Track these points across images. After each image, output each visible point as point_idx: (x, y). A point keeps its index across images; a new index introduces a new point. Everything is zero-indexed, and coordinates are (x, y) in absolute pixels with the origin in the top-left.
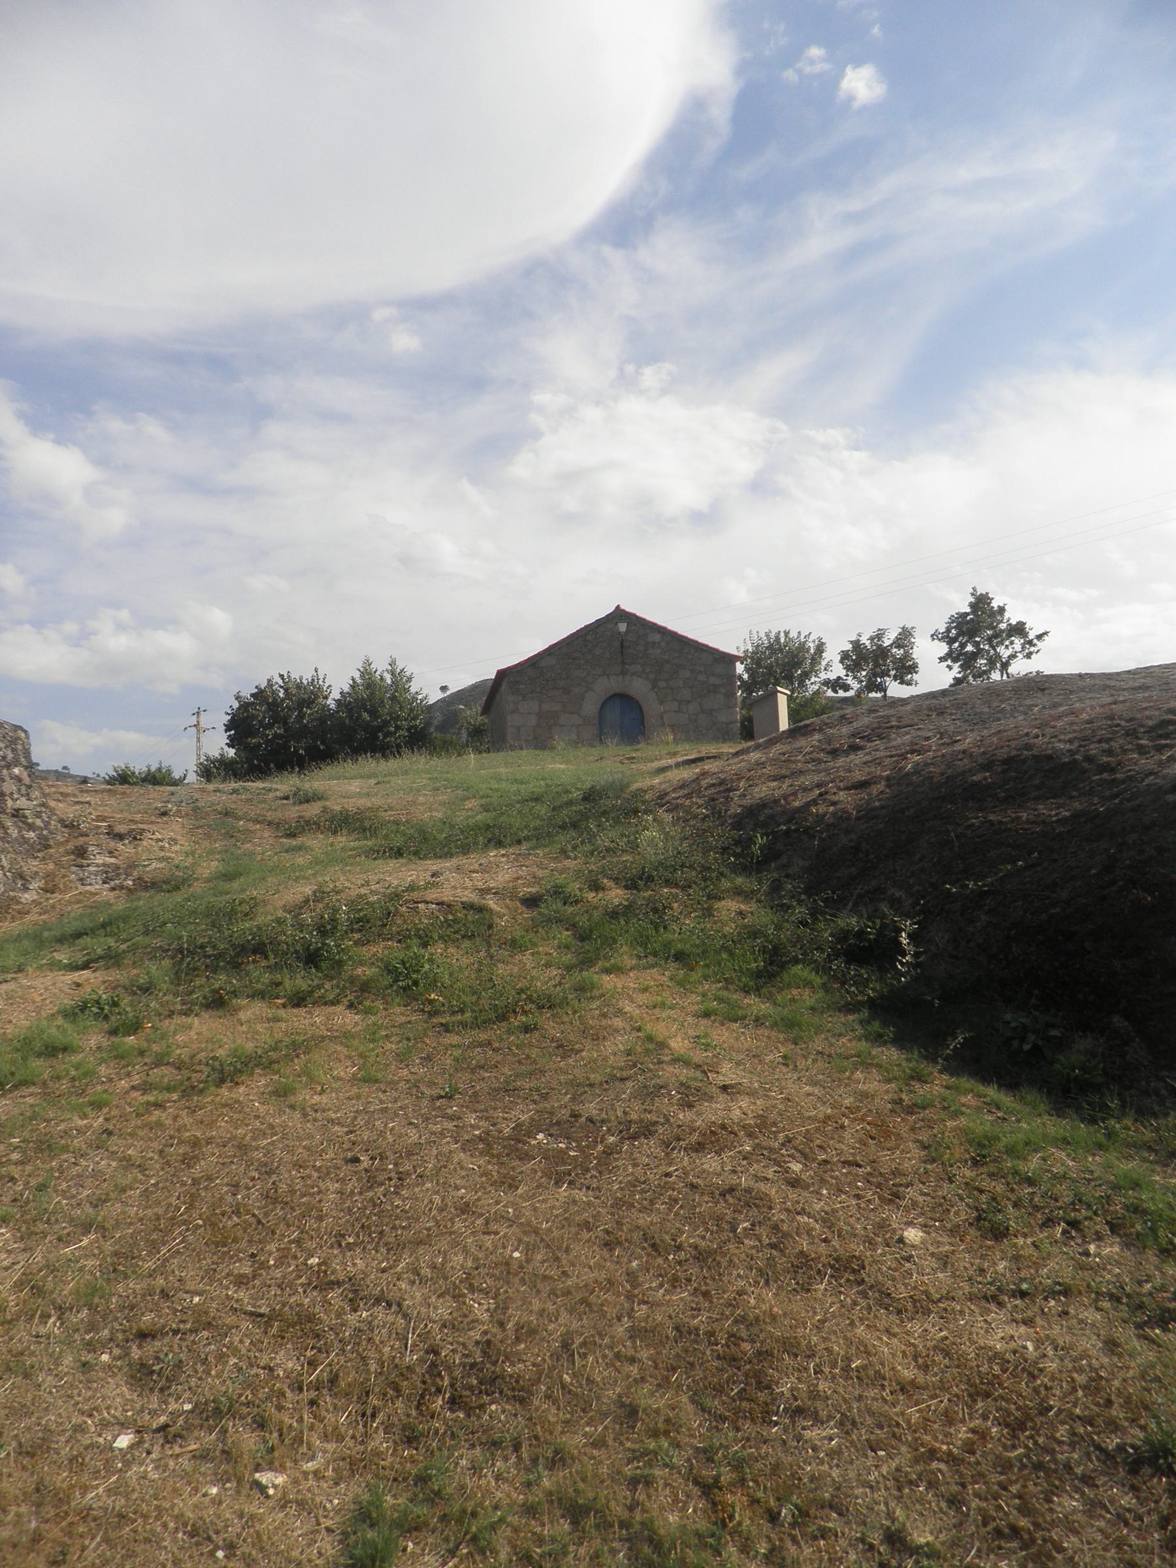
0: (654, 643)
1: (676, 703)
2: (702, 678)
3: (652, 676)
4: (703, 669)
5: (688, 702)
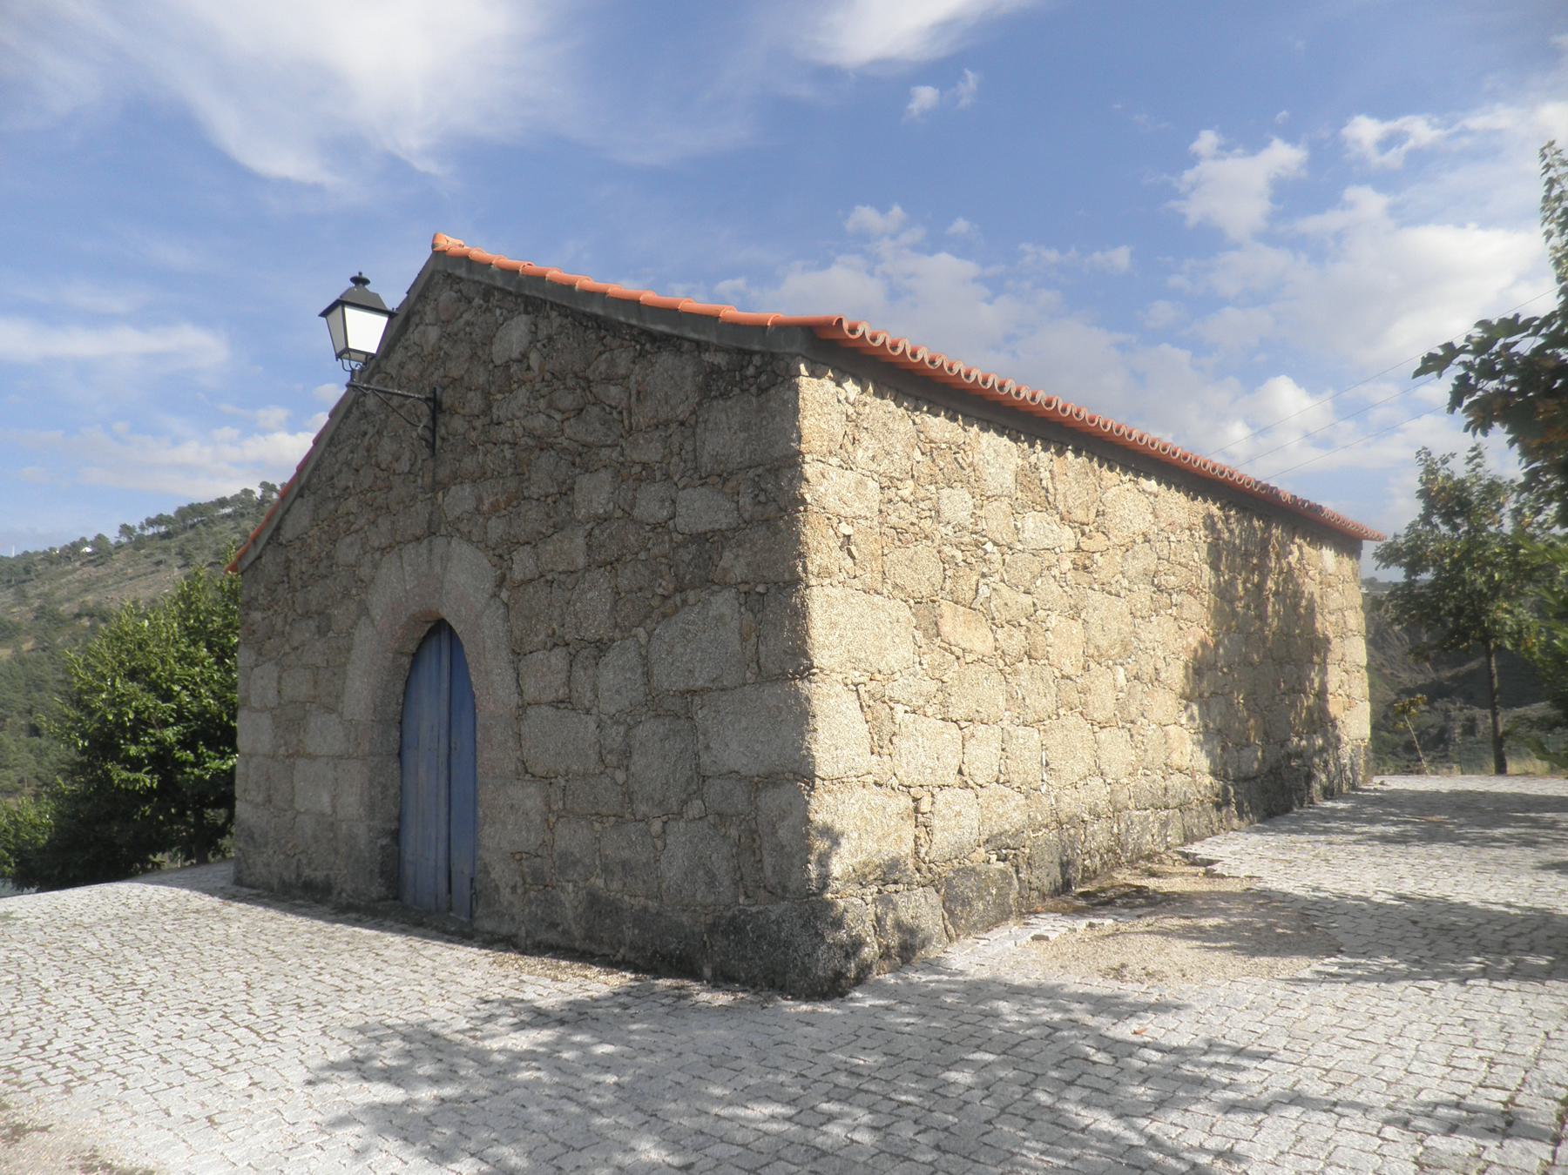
0: (507, 366)
1: (558, 658)
2: (650, 505)
3: (496, 528)
4: (649, 451)
5: (601, 647)
